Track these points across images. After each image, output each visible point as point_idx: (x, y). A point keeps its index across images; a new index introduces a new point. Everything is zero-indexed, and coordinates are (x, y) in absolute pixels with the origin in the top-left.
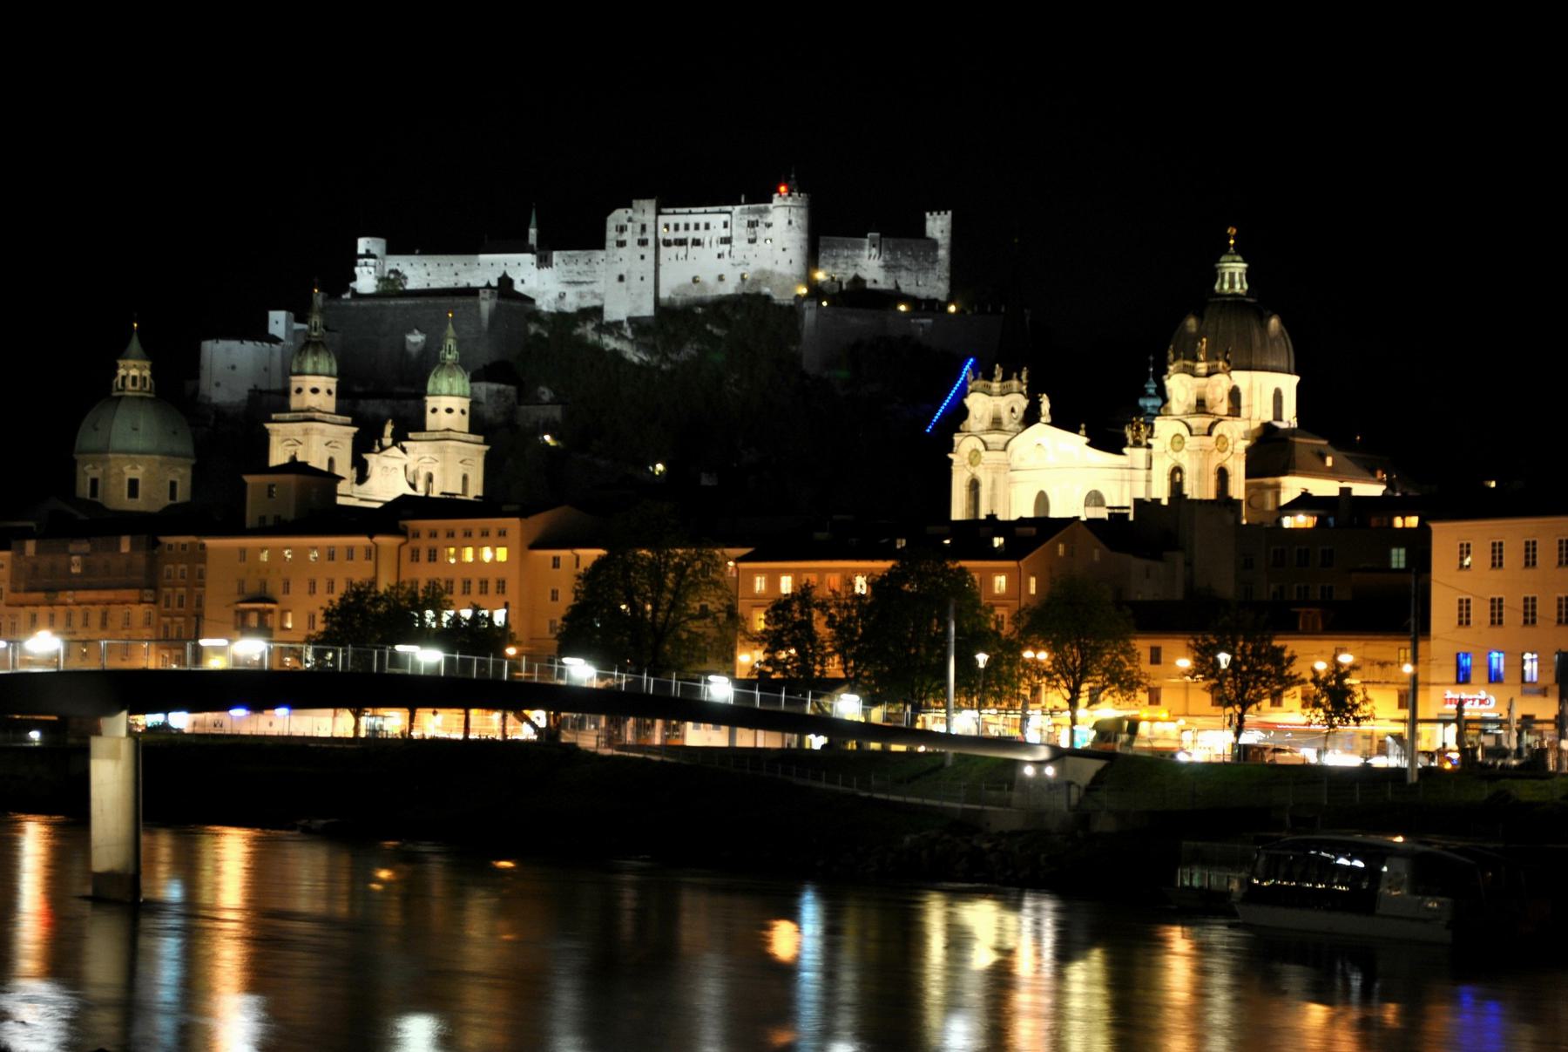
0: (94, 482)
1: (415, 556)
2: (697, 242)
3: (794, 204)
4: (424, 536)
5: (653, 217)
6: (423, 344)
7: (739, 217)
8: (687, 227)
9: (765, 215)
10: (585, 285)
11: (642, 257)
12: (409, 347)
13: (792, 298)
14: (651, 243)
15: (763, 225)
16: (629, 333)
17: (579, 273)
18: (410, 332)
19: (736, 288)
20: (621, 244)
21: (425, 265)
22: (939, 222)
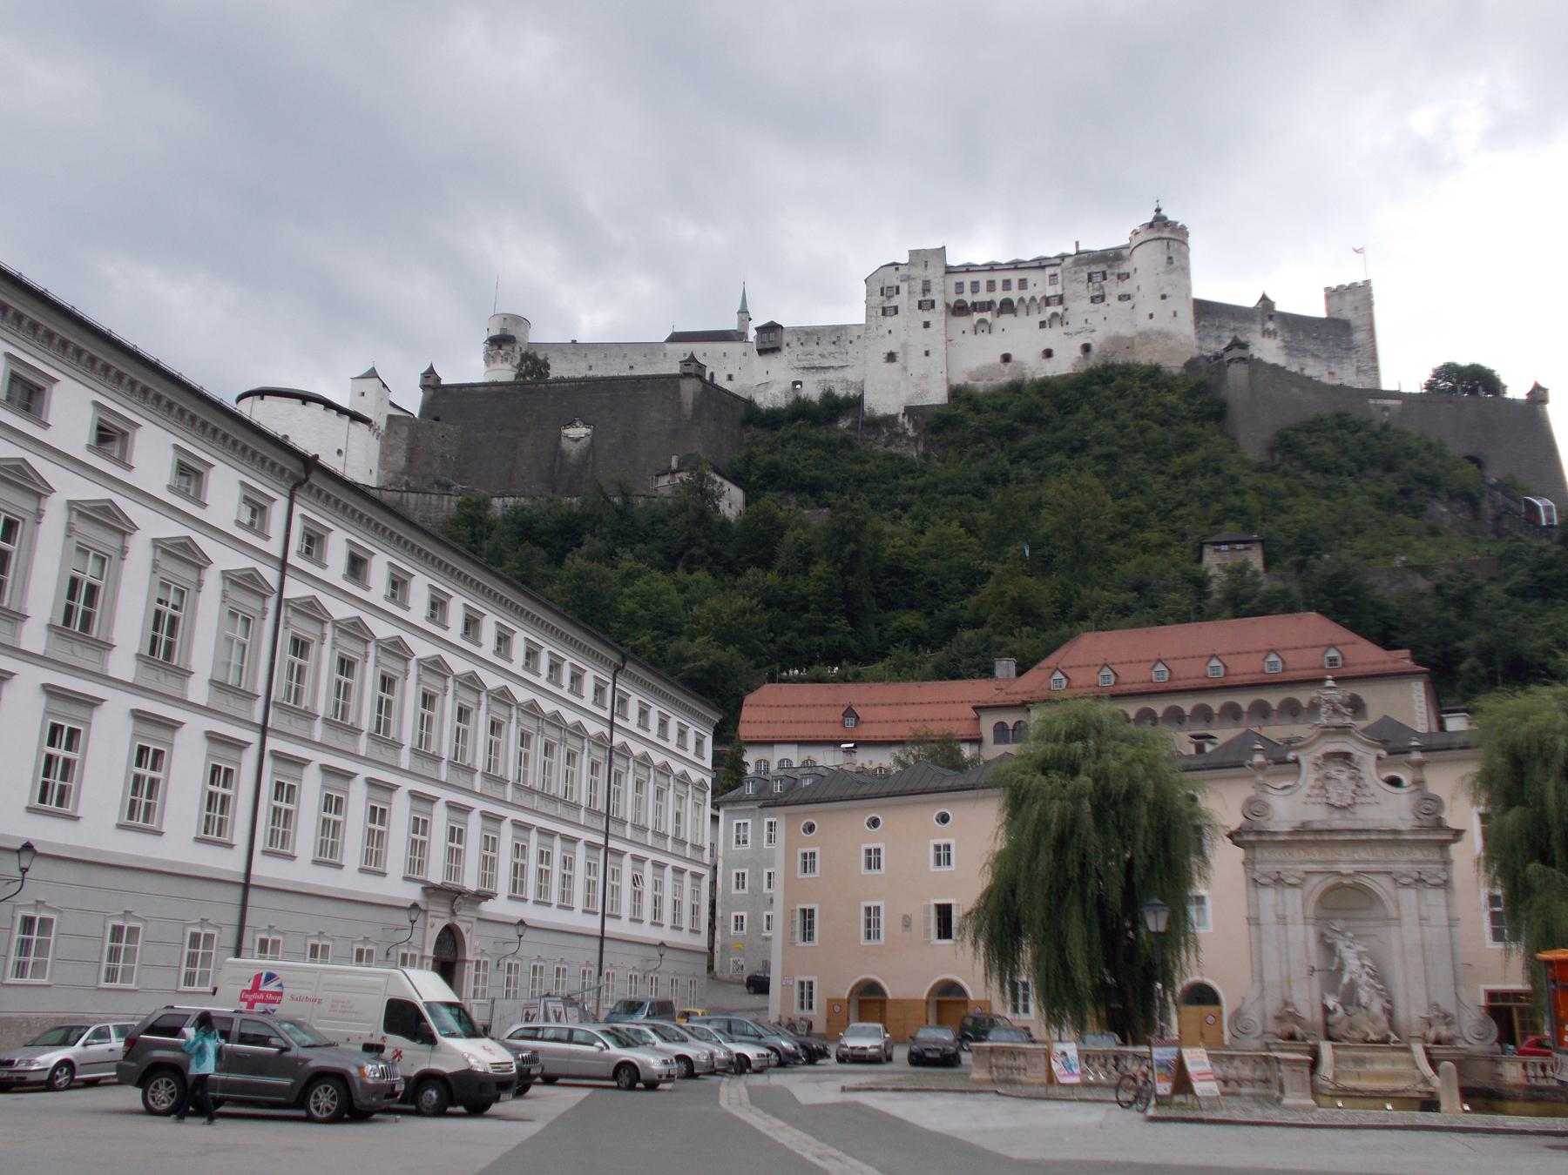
2: (1007, 307)
3: (1173, 236)
5: (942, 271)
6: (588, 439)
7: (1072, 271)
8: (991, 285)
9: (1117, 263)
10: (831, 370)
11: (927, 325)
13: (1181, 365)
14: (940, 306)
15: (1115, 278)
17: (822, 356)
18: (571, 424)
19: (1074, 365)
21: (586, 356)
22: (1349, 298)
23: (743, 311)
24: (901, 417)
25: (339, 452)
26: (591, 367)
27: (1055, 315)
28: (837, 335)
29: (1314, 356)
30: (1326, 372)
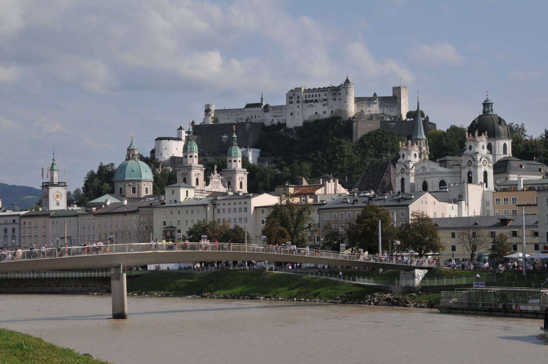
0: (121, 189)
1: (219, 211)
2: (316, 101)
4: (221, 204)
6: (227, 138)
8: (313, 96)
11: (298, 107)
12: (223, 140)
15: (338, 94)
16: (295, 131)
17: (278, 113)
18: (224, 135)
19: (330, 116)
20: (291, 103)
22: (397, 90)
23: (262, 99)
24: (293, 129)
25: (177, 149)
26: (229, 115)
27: (326, 103)
28: (281, 107)
29: (387, 107)
30: (389, 111)
